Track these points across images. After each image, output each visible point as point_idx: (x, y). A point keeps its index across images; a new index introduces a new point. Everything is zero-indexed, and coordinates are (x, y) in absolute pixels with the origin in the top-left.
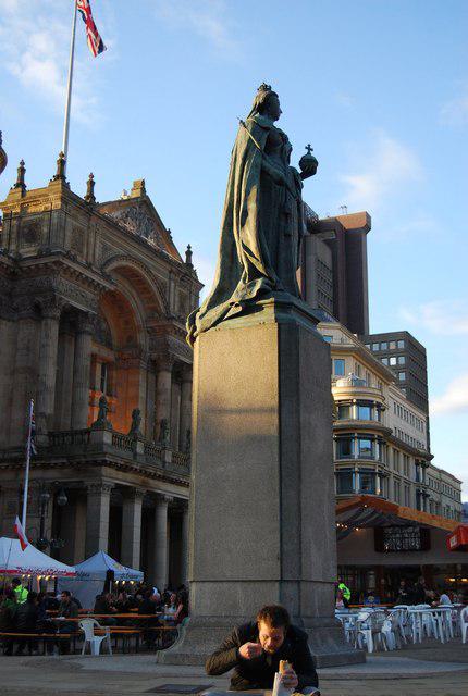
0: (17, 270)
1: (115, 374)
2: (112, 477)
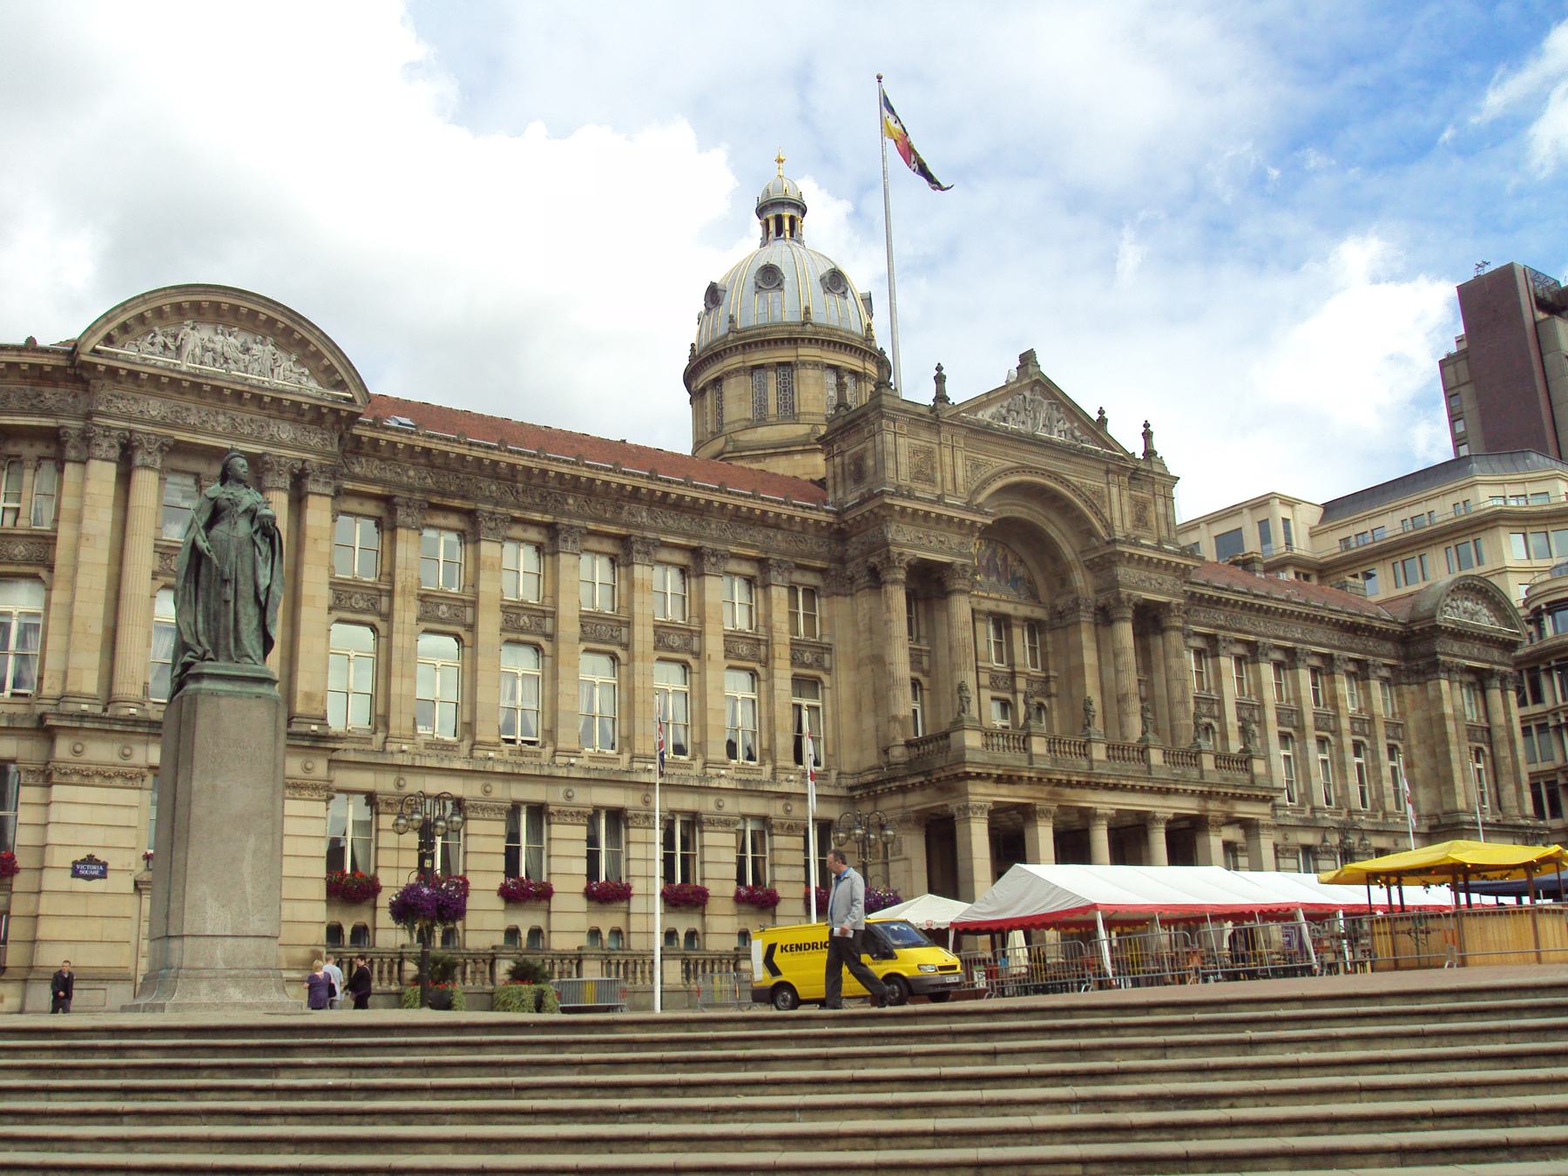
0: (843, 526)
1: (1049, 638)
2: (982, 795)
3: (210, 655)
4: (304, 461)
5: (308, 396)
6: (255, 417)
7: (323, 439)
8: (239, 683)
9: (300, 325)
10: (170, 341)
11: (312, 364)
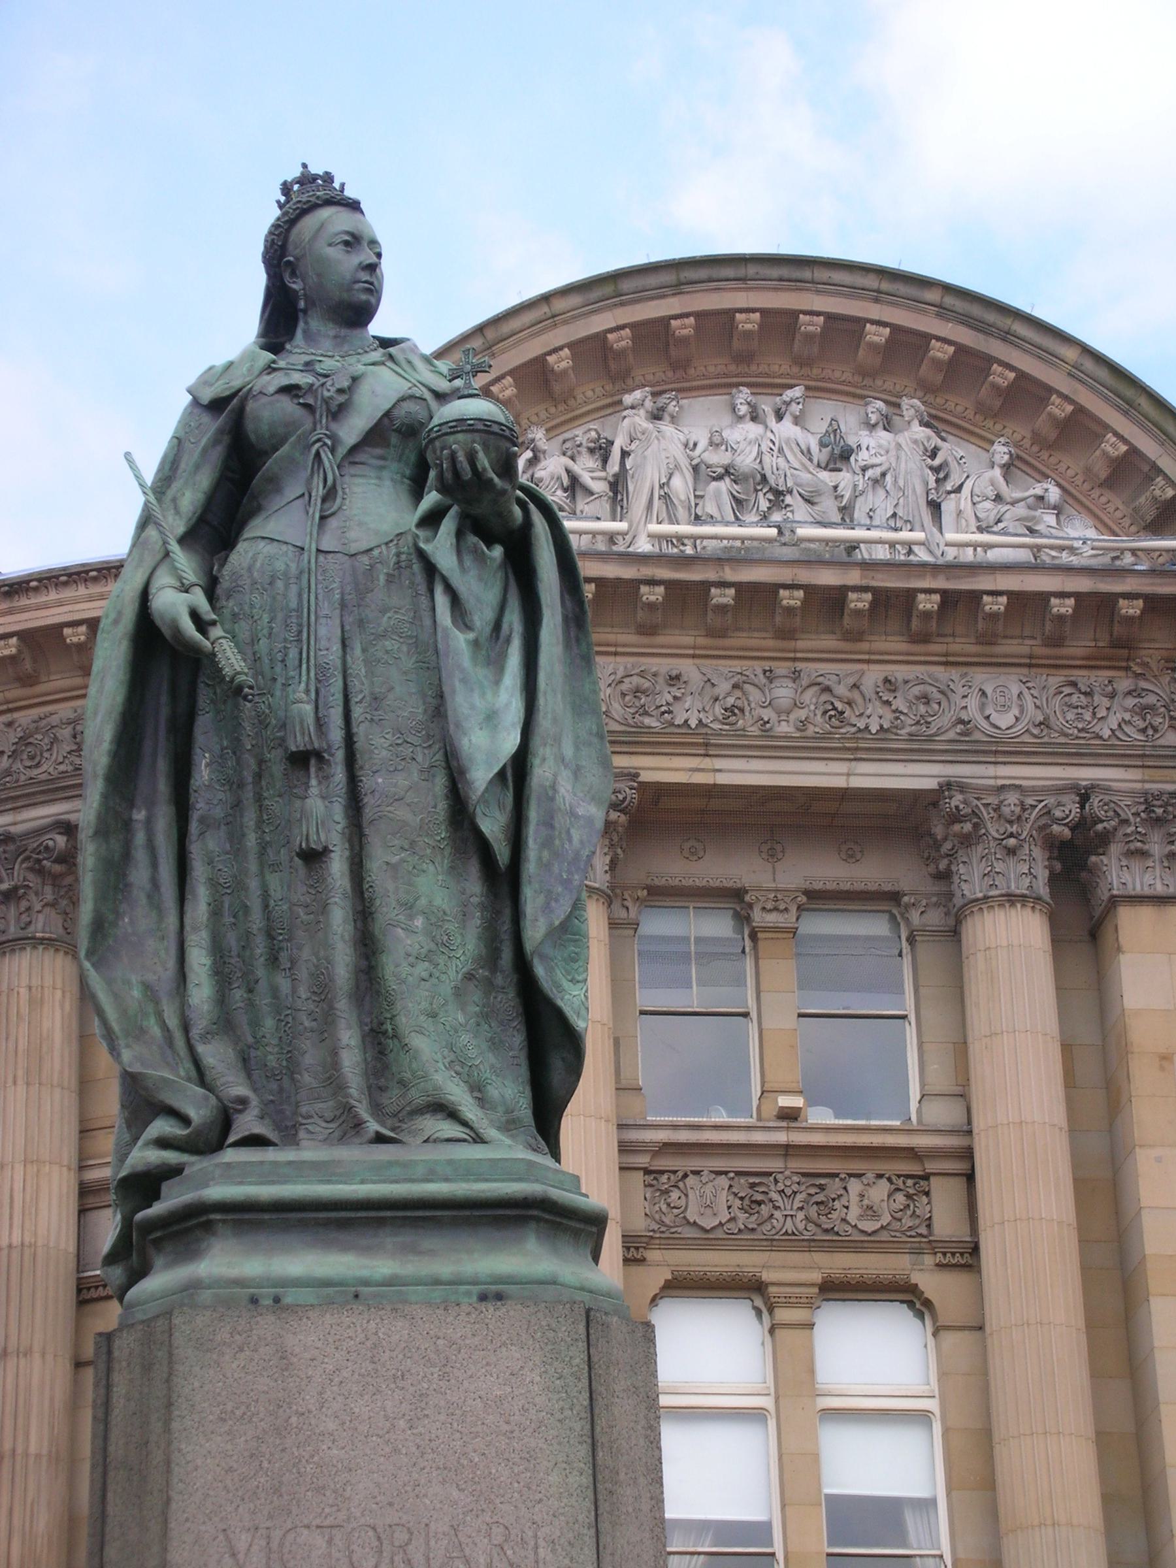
3: (248, 1123)
4: (1084, 795)
5: (1069, 570)
6: (900, 672)
7: (1143, 710)
8: (390, 1239)
9: (1006, 337)
10: (586, 468)
11: (1071, 464)
